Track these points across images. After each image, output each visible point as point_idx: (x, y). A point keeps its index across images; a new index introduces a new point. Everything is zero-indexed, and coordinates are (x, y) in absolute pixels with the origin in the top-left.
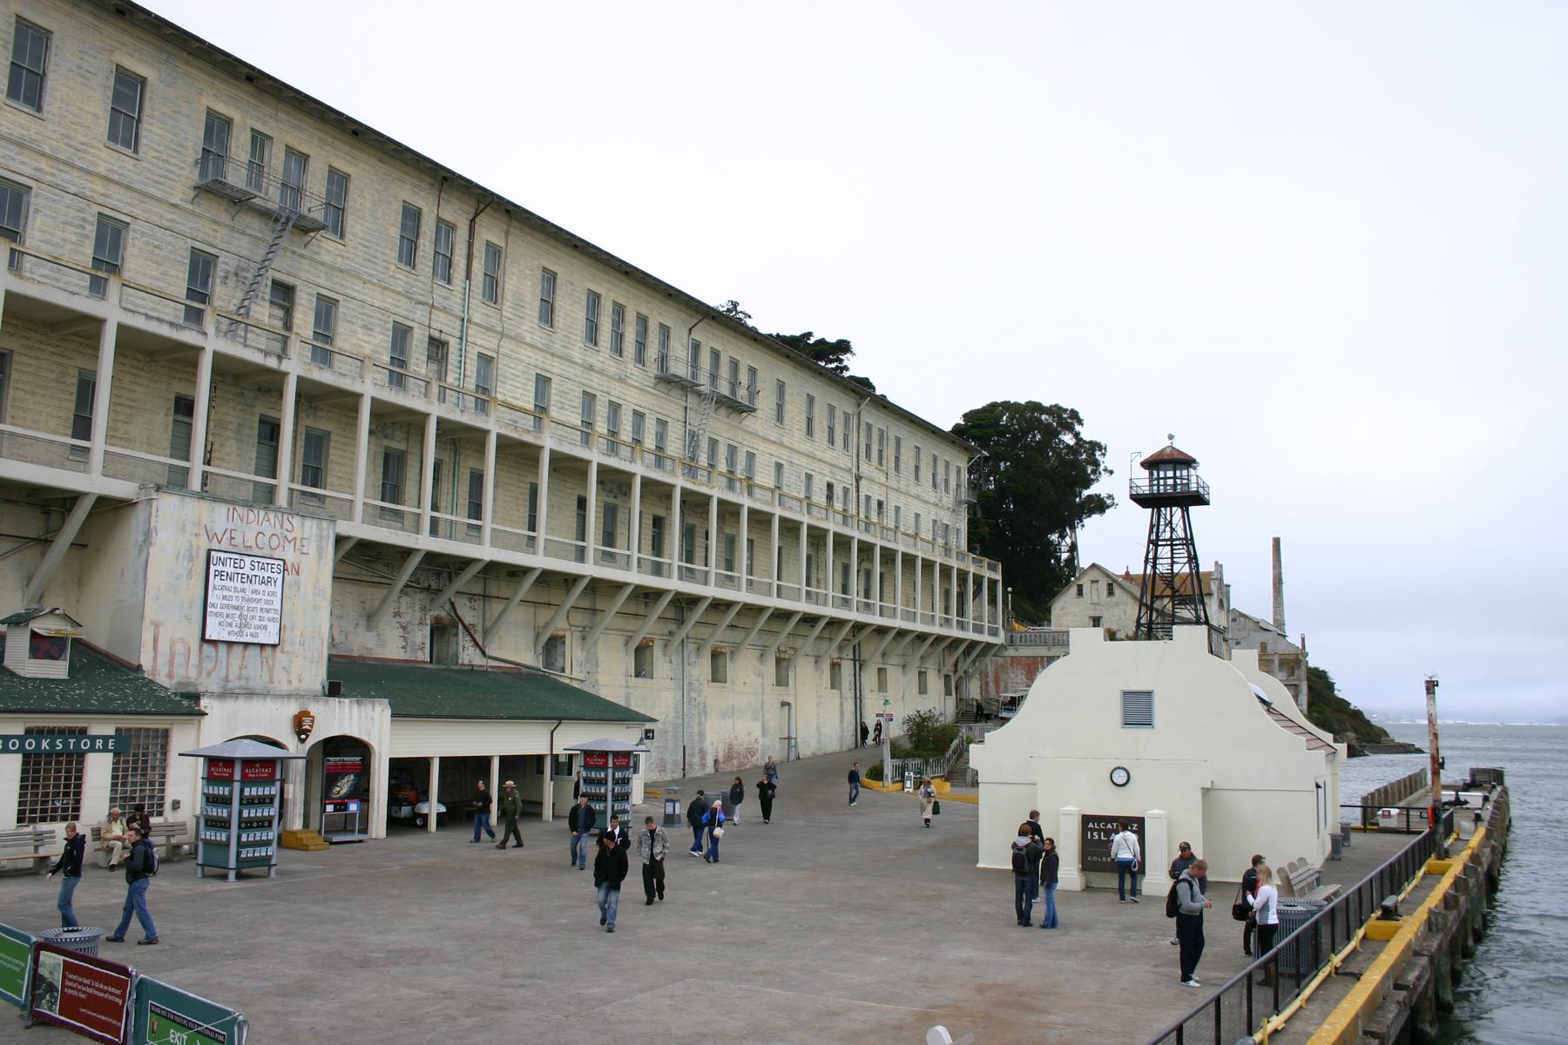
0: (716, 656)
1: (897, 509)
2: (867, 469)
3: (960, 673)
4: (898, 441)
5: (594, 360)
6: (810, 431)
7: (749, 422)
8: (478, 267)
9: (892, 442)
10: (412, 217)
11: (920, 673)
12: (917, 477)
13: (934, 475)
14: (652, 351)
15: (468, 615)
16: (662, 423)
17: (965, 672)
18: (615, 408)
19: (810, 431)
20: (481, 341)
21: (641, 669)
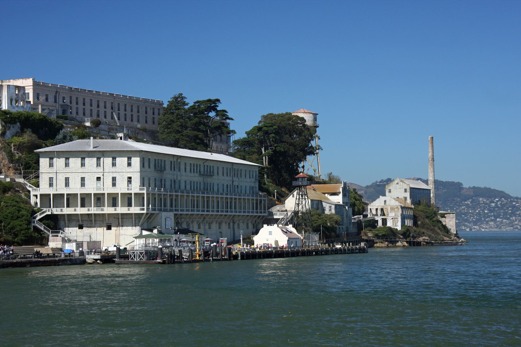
0: (209, 223)
1: (241, 186)
2: (234, 179)
3: (257, 223)
4: (241, 170)
5: (191, 175)
6: (223, 175)
7: (214, 177)
8: (178, 166)
9: (240, 171)
10: (171, 162)
11: (247, 224)
12: (246, 177)
13: (250, 175)
14: (198, 170)
15: (180, 221)
16: (200, 183)
17: (258, 223)
18: (194, 182)
19: (223, 175)
20: (179, 178)
21: (199, 228)
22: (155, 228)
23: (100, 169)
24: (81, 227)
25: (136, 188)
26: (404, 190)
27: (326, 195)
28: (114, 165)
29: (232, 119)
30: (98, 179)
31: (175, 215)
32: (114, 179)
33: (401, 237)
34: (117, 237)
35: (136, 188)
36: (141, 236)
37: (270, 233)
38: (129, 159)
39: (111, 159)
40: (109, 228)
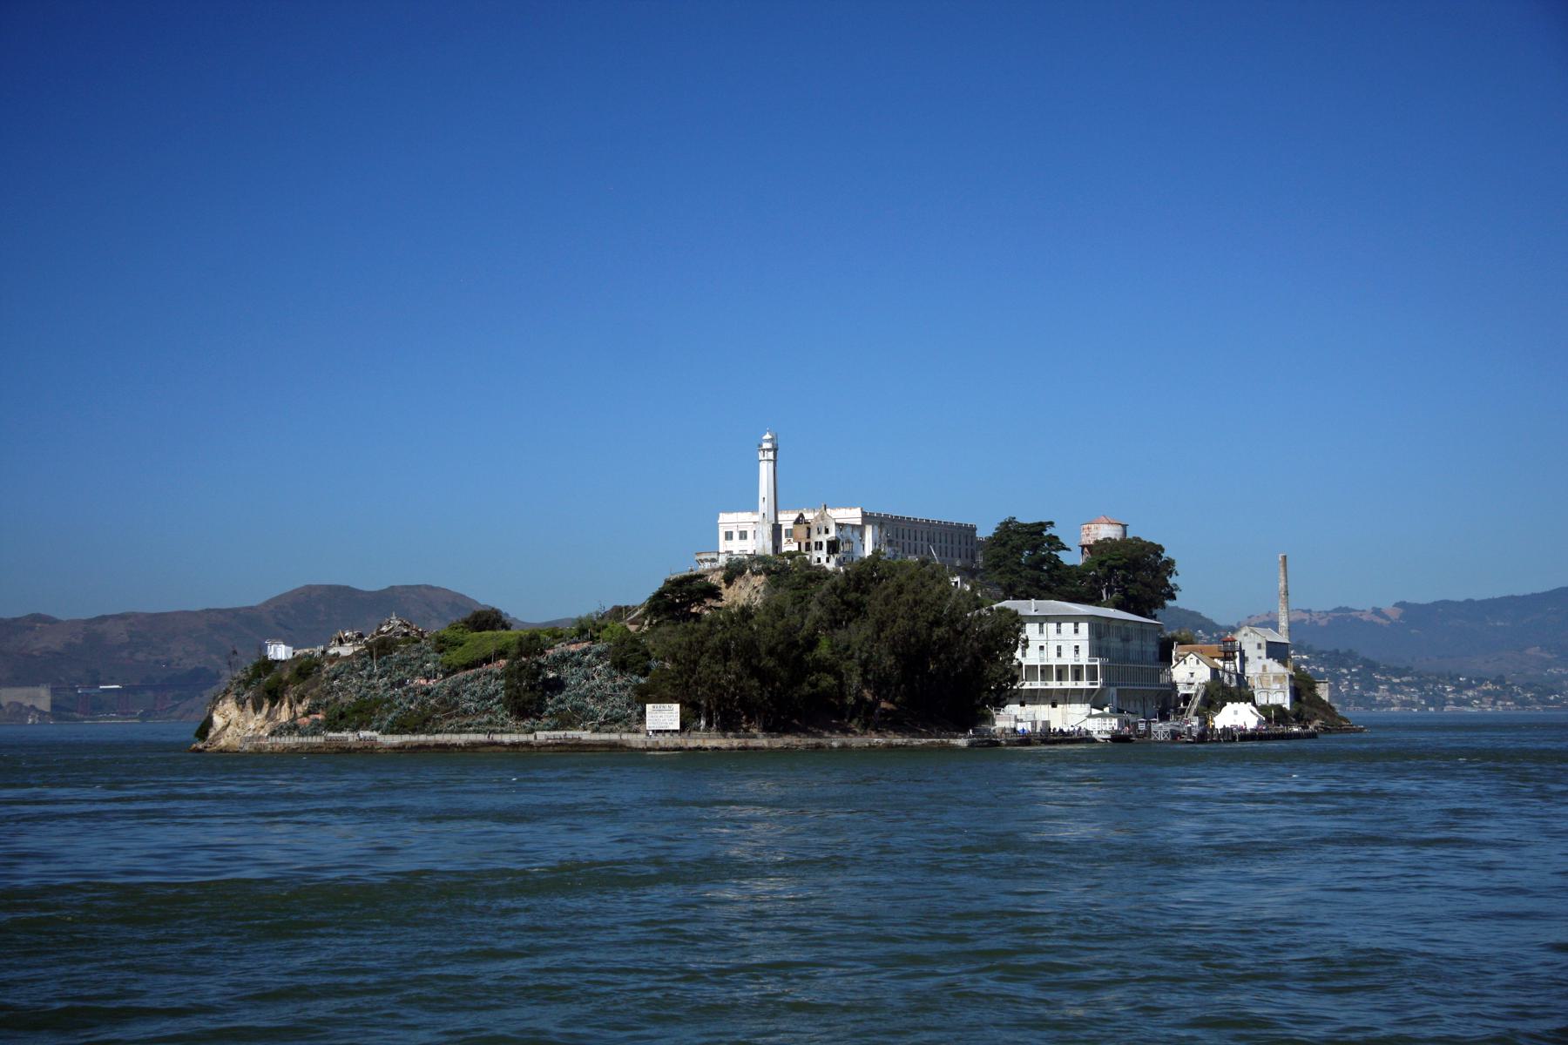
22: (1106, 705)
23: (1044, 637)
24: (1022, 704)
25: (1084, 659)
26: (1256, 646)
27: (1216, 660)
28: (1059, 631)
29: (1069, 550)
30: (1042, 648)
31: (1118, 690)
32: (1059, 648)
33: (1294, 720)
34: (1064, 715)
35: (1084, 659)
36: (1090, 716)
37: (1236, 713)
38: (1076, 624)
39: (1055, 624)
40: (1054, 705)
